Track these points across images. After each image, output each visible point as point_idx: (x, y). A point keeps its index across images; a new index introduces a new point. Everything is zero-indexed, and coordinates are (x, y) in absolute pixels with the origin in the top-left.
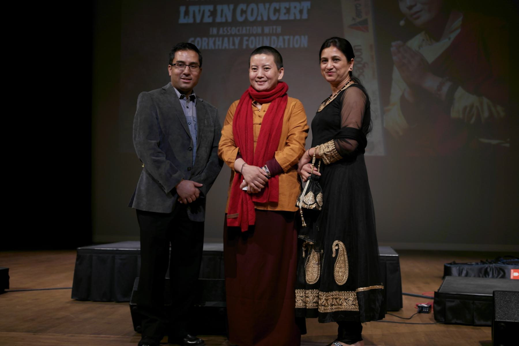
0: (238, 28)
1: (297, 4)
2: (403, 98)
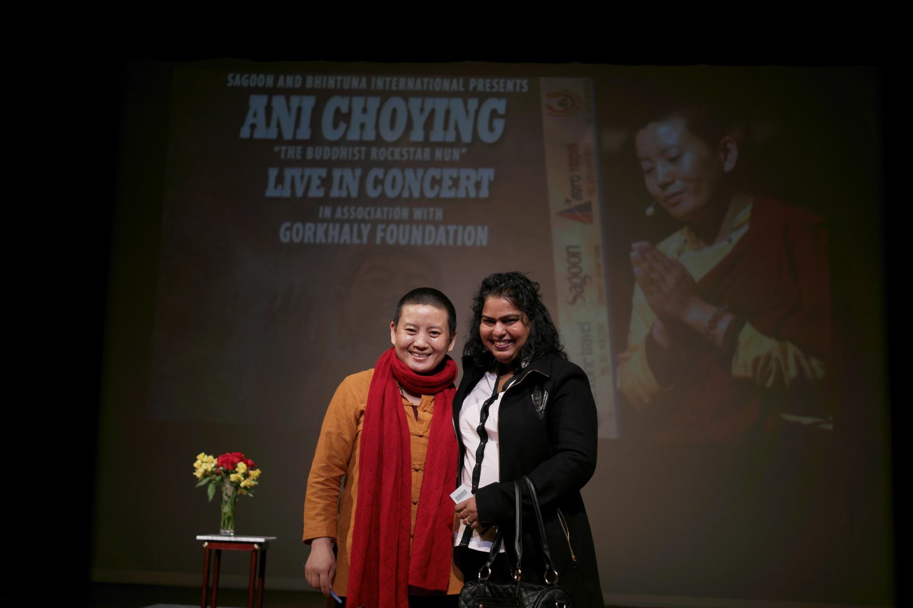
0: (368, 209)
1: (471, 173)
2: (650, 339)
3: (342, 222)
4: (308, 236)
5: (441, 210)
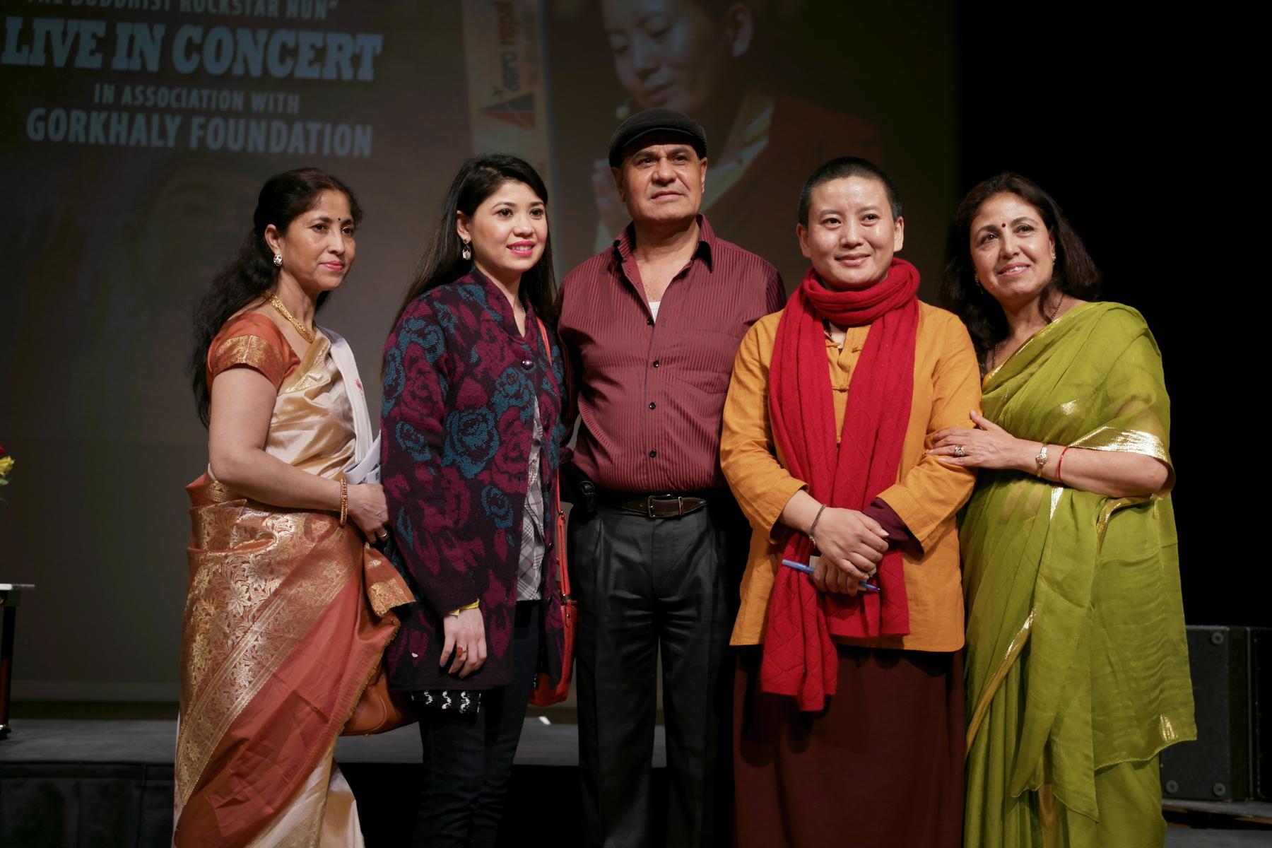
0: (176, 91)
1: (345, 39)
3: (133, 111)
4: (76, 132)
5: (297, 97)
